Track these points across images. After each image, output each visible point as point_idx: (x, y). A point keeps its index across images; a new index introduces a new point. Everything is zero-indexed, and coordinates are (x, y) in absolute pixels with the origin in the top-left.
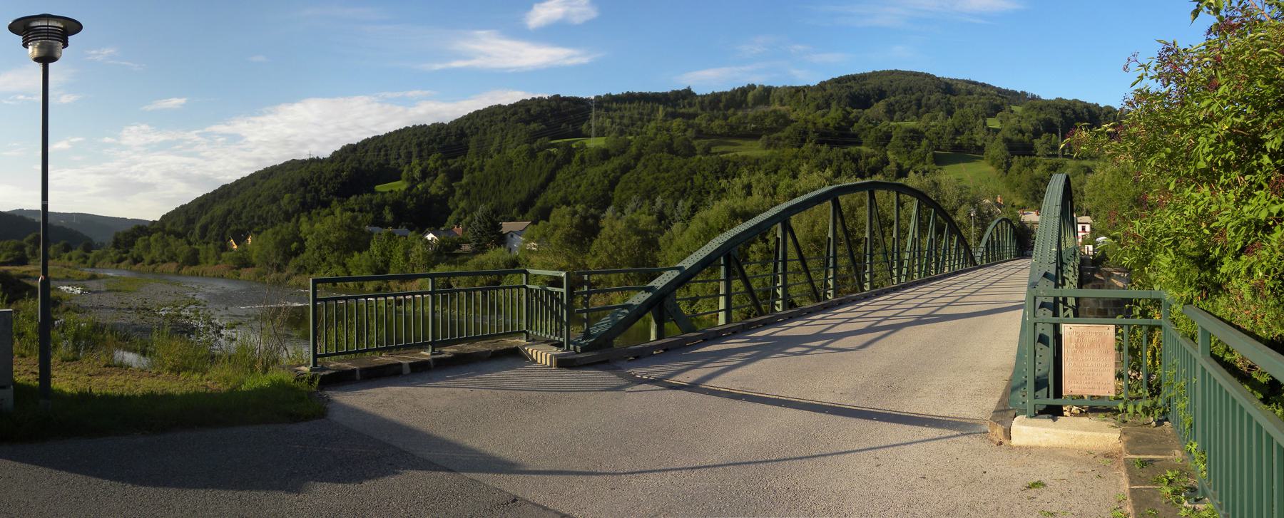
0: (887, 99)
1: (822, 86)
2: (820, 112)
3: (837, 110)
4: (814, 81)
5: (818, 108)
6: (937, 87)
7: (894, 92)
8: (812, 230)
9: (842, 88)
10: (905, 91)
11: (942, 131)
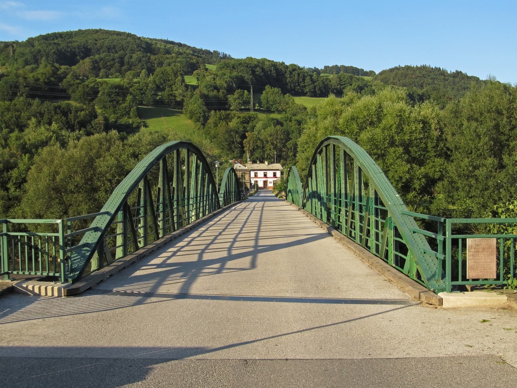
0: (92, 57)
1: (31, 42)
2: (28, 67)
3: (46, 66)
4: (23, 38)
5: (27, 63)
6: (138, 47)
7: (98, 50)
8: (54, 179)
9: (50, 44)
10: (109, 49)
11: (145, 87)
